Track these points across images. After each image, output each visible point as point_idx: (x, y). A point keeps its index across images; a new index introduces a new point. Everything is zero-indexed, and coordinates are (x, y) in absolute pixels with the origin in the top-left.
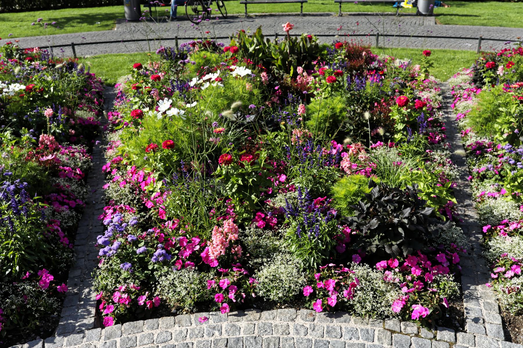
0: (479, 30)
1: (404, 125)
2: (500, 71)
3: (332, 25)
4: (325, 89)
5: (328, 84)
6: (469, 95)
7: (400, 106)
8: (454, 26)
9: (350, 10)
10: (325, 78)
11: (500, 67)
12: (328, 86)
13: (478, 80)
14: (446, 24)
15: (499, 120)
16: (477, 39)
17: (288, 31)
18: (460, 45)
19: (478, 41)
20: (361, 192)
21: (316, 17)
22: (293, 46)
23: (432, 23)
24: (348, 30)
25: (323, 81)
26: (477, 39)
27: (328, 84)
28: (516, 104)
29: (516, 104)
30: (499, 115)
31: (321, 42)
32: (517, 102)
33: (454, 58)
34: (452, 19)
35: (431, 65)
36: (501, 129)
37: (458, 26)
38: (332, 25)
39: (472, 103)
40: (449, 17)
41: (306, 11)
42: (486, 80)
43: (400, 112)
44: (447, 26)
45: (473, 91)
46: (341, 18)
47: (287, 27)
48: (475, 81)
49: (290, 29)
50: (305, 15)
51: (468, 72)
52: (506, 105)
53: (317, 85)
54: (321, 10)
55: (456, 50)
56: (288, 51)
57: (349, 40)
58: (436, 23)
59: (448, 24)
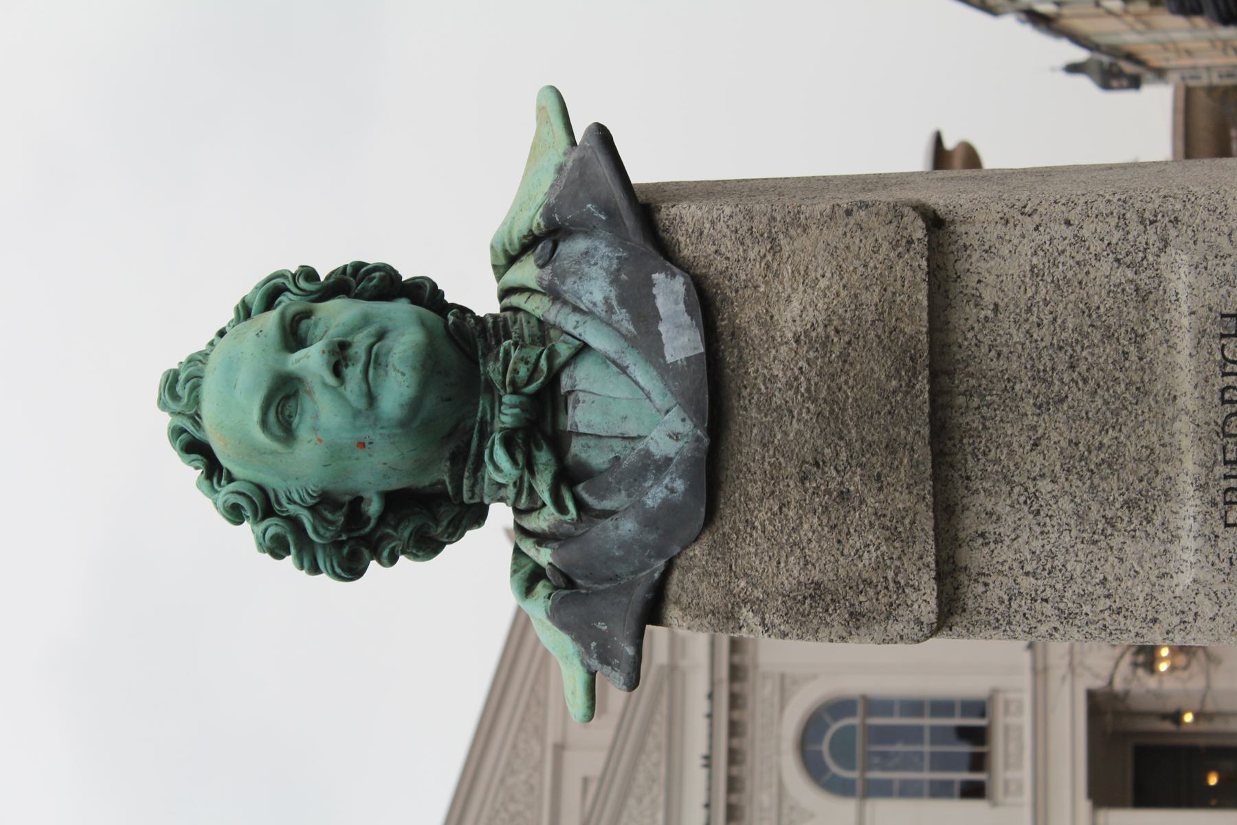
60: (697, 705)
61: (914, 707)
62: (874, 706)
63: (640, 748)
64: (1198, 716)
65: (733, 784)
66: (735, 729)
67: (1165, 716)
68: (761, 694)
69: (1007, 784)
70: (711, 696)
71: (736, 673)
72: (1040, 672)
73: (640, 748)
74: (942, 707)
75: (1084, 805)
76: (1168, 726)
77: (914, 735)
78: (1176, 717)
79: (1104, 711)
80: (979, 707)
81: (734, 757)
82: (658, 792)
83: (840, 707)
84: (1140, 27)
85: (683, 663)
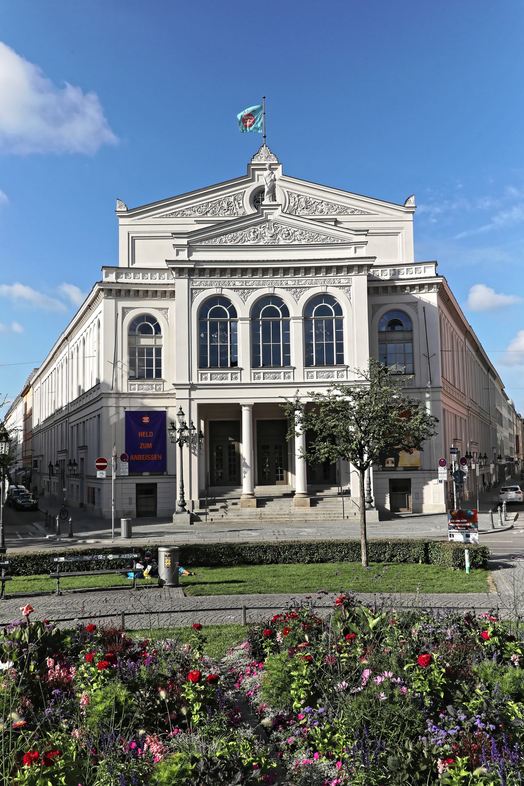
0: (238, 599)
1: (200, 704)
2: (279, 637)
3: (51, 608)
4: (97, 678)
5: (99, 671)
6: (251, 671)
7: (193, 682)
8: (208, 597)
9: (70, 586)
10: (93, 665)
11: (279, 634)
12: (99, 674)
13: (257, 654)
14: (198, 595)
15: (294, 686)
16: (241, 609)
17: (27, 615)
18: (222, 618)
19: (241, 612)
20: (186, 770)
21: (25, 599)
22: (32, 635)
23: (181, 596)
24: (77, 612)
25: (93, 669)
26: (241, 609)
27: (99, 671)
28: (306, 664)
29: (306, 664)
30: (292, 679)
31: (62, 627)
32: (306, 662)
33: (220, 634)
34: (203, 589)
35: (204, 641)
36: (297, 694)
37: (212, 596)
38: (51, 608)
39: (259, 676)
40: (199, 587)
41: (8, 593)
42: (267, 650)
43: (194, 689)
44: (199, 597)
45: (254, 666)
46: (60, 597)
47: (27, 610)
48: (254, 654)
49: (30, 612)
50: (8, 598)
51: (242, 646)
52: (296, 667)
53: (86, 675)
54: (29, 589)
55: (219, 624)
56: (27, 641)
57: (95, 622)
58: (185, 596)
59: (201, 595)
61: (340, 336)
68: (342, 278)
71: (350, 269)
74: (340, 348)
77: (330, 337)
80: (341, 360)
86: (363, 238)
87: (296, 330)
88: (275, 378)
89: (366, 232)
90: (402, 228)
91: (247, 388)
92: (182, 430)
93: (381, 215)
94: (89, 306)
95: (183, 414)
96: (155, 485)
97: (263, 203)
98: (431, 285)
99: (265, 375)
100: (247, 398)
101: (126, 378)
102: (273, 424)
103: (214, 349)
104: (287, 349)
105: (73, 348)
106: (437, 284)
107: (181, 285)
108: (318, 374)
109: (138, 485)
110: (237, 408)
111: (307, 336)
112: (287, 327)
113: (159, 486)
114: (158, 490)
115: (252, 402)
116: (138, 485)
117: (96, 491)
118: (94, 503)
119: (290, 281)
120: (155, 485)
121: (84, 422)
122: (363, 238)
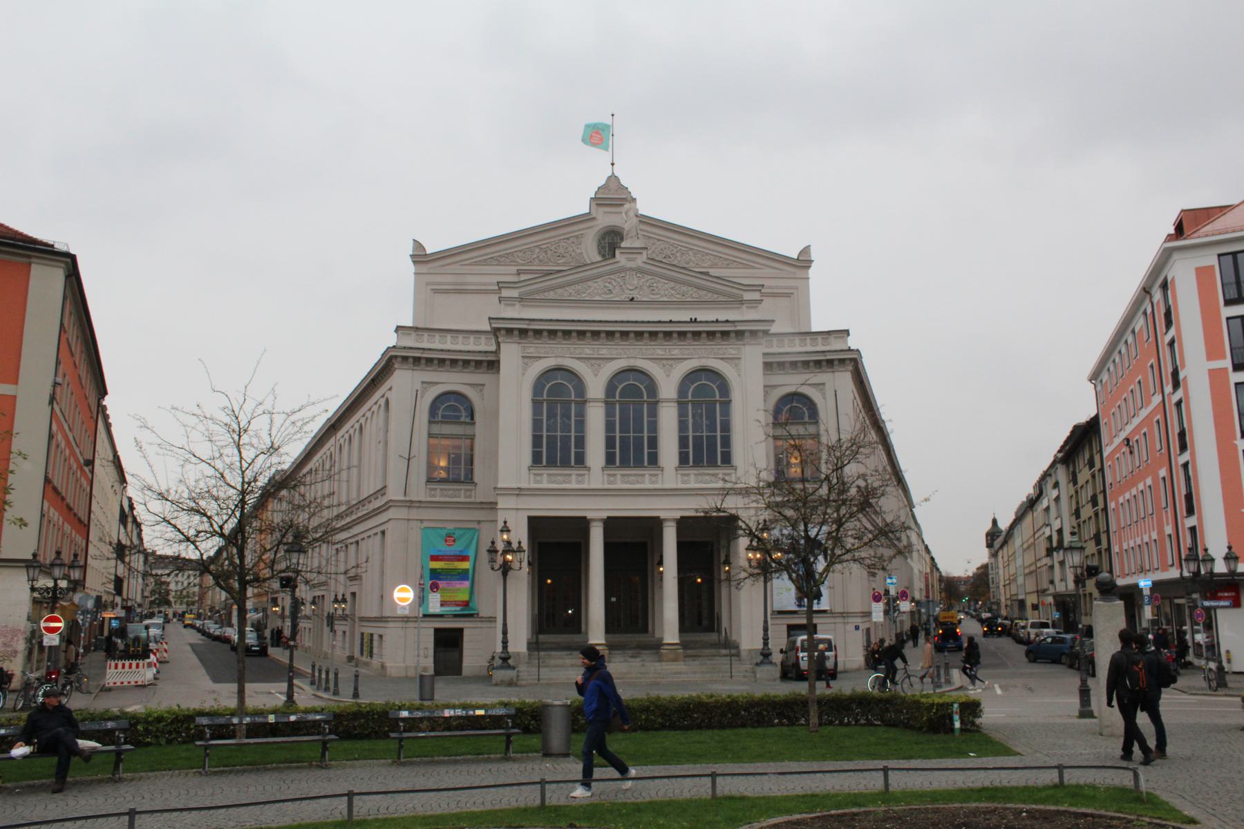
60: (722, 316)
61: (726, 427)
62: (726, 404)
63: (699, 288)
64: (728, 572)
65: (682, 335)
66: (711, 334)
67: (728, 556)
68: (730, 349)
69: (688, 475)
70: (727, 321)
72: (746, 492)
73: (699, 288)
74: (727, 442)
75: (678, 515)
76: (723, 559)
77: (712, 428)
78: (727, 562)
79: (726, 525)
80: (727, 459)
81: (696, 335)
82: (678, 297)
83: (724, 388)
84: (1025, 546)
85: (744, 307)
86: (756, 296)
87: (668, 419)
88: (638, 482)
89: (758, 288)
90: (797, 288)
91: (597, 494)
92: (505, 552)
93: (767, 271)
94: (373, 380)
95: (508, 531)
96: (461, 631)
97: (623, 245)
98: (842, 361)
99: (622, 479)
100: (597, 510)
101: (424, 479)
102: (632, 544)
103: (552, 441)
104: (653, 442)
105: (342, 441)
106: (851, 360)
107: (510, 353)
108: (695, 479)
109: (437, 631)
110: (581, 525)
111: (682, 426)
112: (653, 413)
113: (466, 632)
114: (466, 638)
115: (605, 515)
116: (437, 631)
117: (376, 637)
118: (371, 654)
119: (659, 349)
120: (461, 631)
121: (357, 542)
122: (756, 296)
